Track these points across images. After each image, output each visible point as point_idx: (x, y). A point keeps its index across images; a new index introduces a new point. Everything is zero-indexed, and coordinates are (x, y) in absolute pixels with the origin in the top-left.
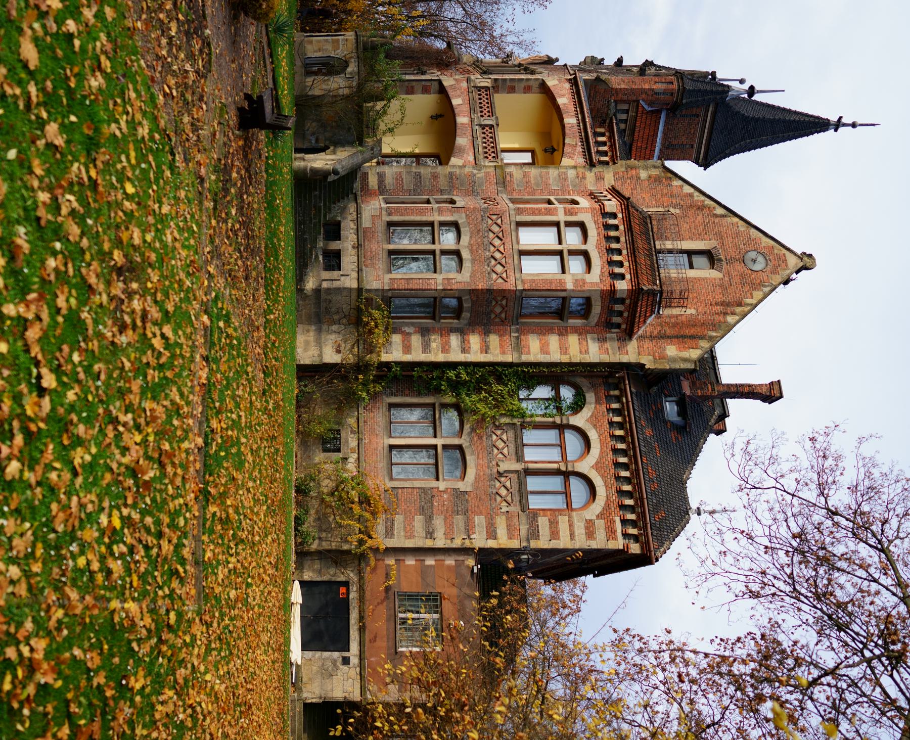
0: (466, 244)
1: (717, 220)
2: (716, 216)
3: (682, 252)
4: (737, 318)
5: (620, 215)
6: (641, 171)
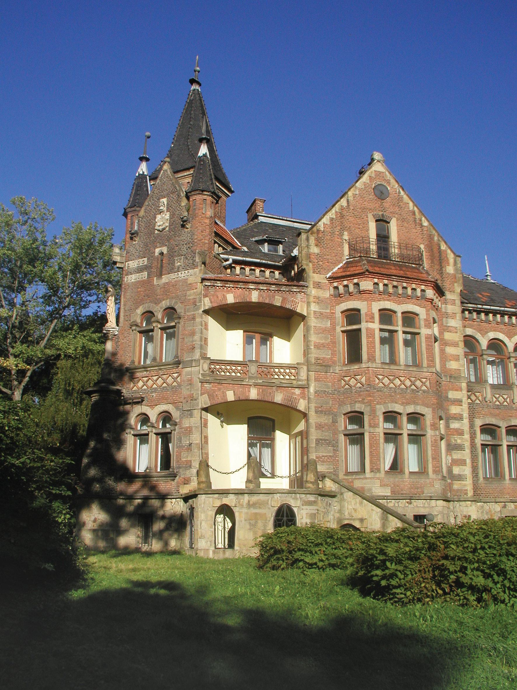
1: (352, 208)
5: (376, 280)
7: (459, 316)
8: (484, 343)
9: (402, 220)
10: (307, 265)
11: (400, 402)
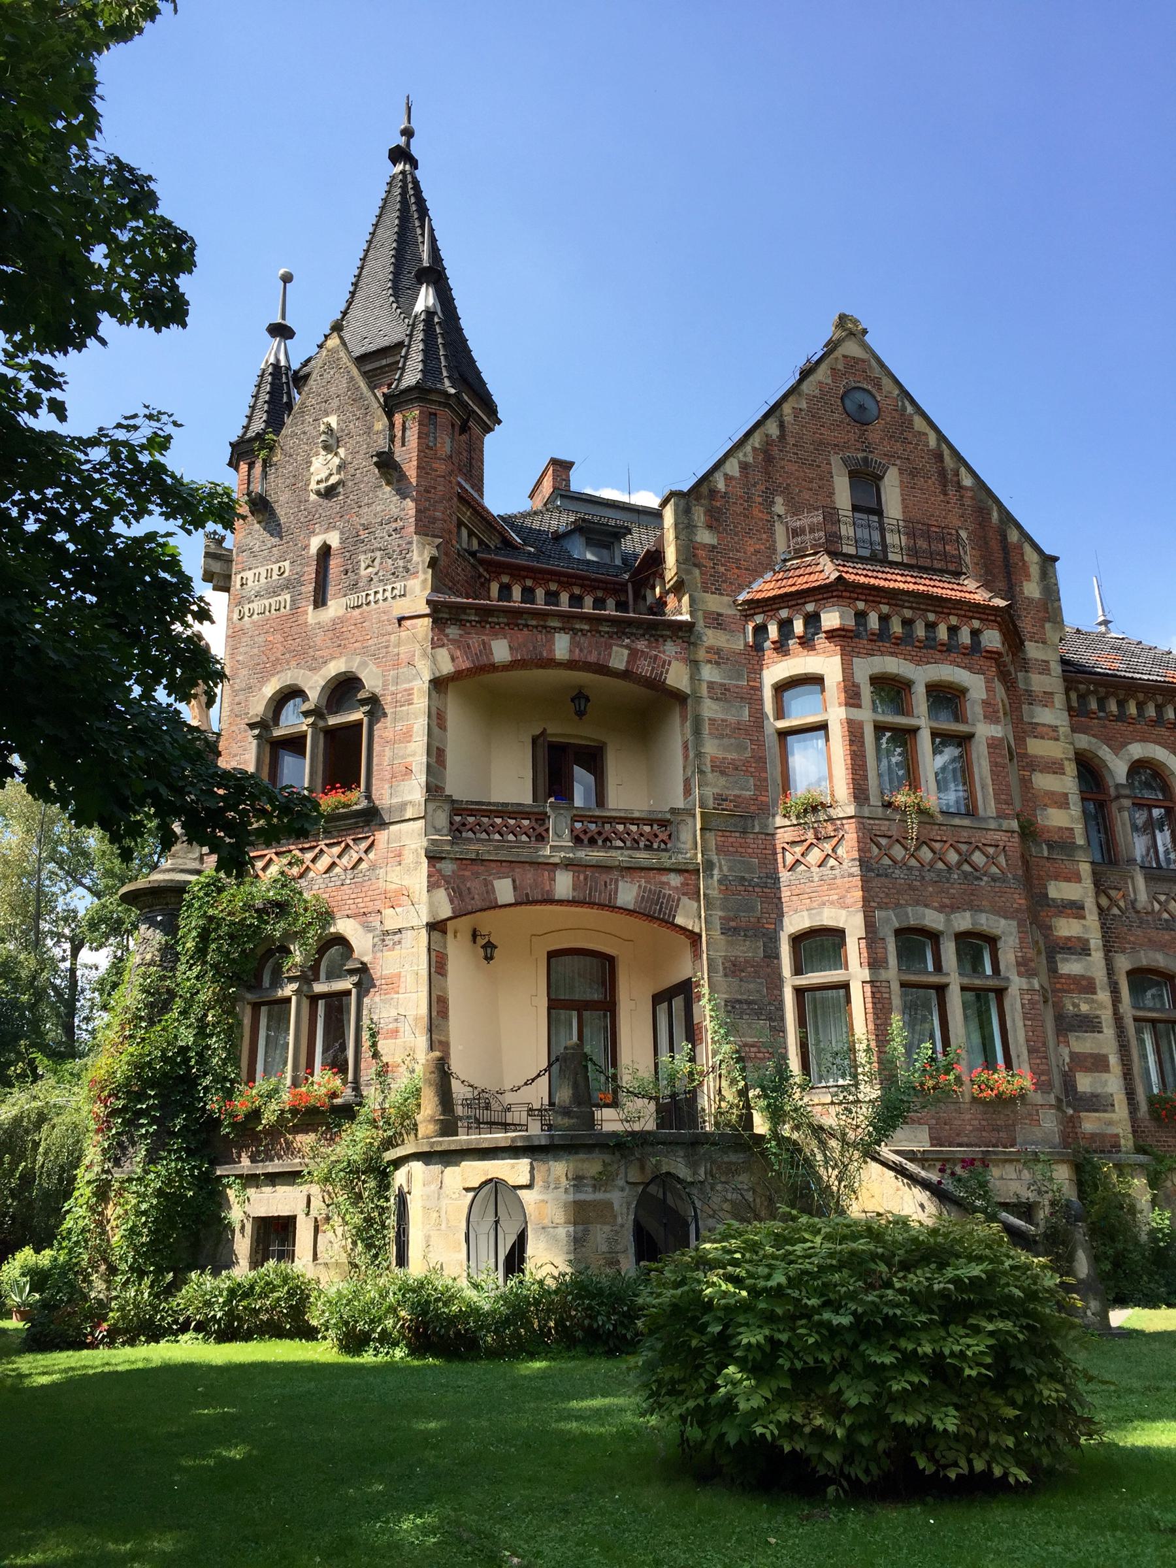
0: (942, 917)
1: (792, 441)
2: (782, 436)
4: (963, 470)
5: (861, 605)
7: (1059, 700)
8: (1118, 768)
9: (911, 474)
11: (936, 904)
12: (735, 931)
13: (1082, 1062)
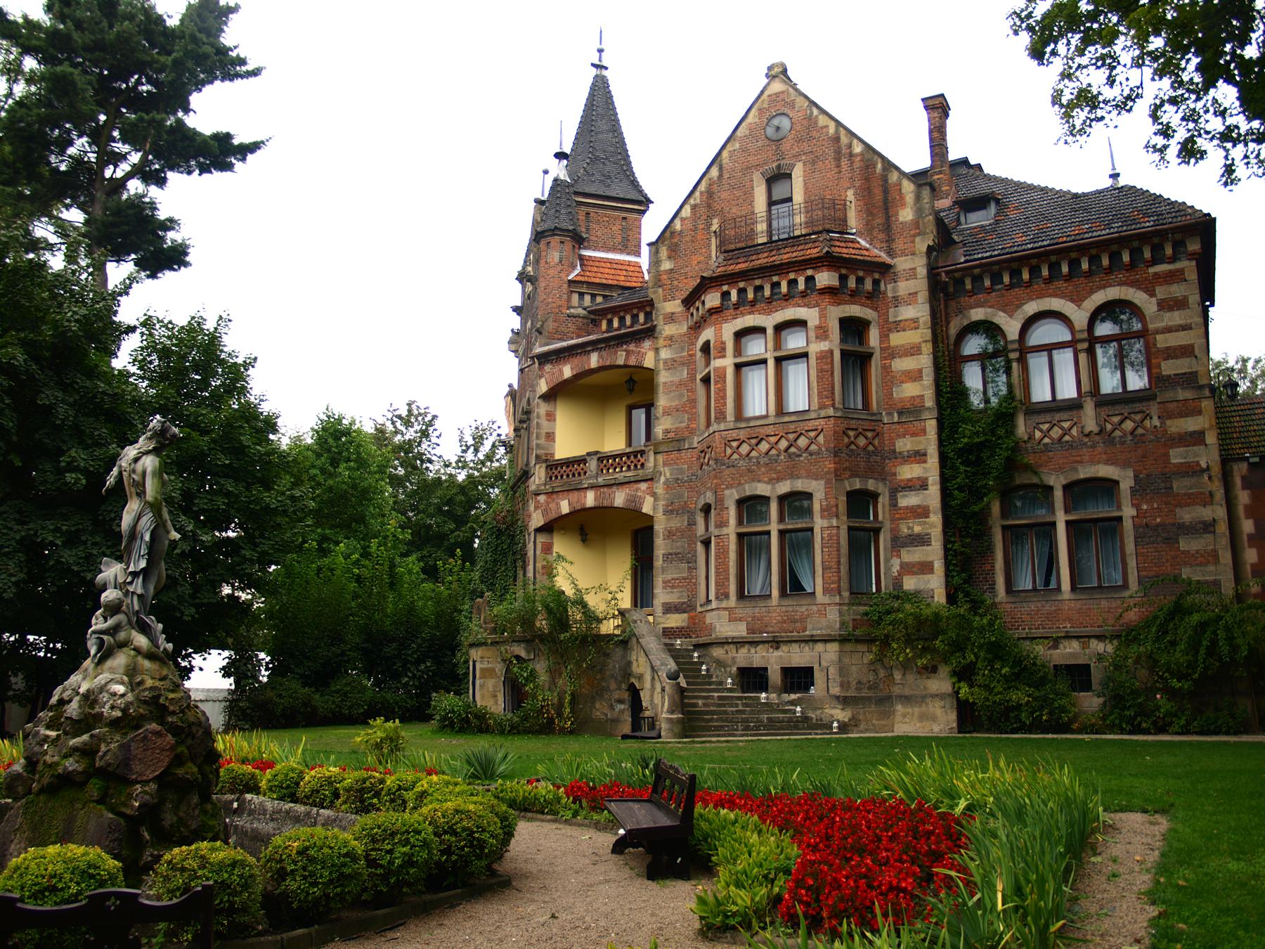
0: (769, 487)
1: (726, 176)
2: (721, 176)
3: (769, 211)
4: (855, 141)
5: (725, 288)
6: (662, 268)
7: (923, 296)
10: (655, 292)
12: (672, 511)
13: (908, 569)
